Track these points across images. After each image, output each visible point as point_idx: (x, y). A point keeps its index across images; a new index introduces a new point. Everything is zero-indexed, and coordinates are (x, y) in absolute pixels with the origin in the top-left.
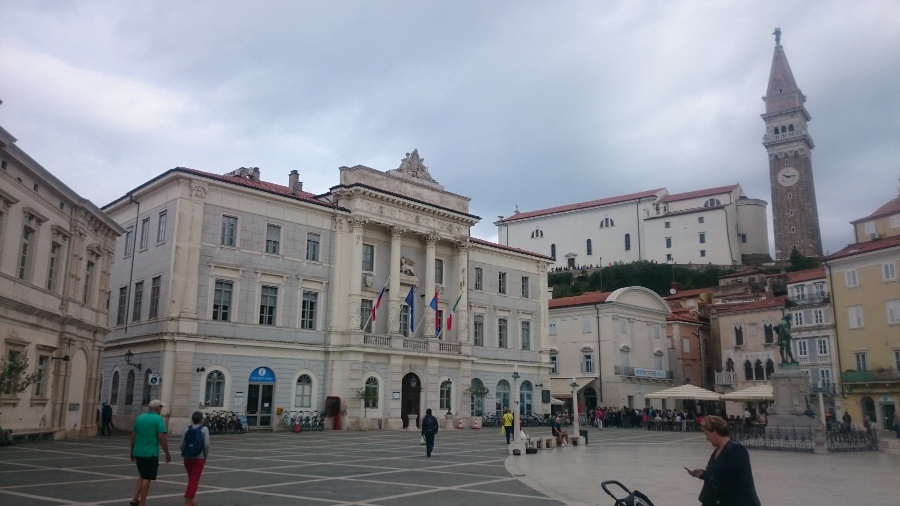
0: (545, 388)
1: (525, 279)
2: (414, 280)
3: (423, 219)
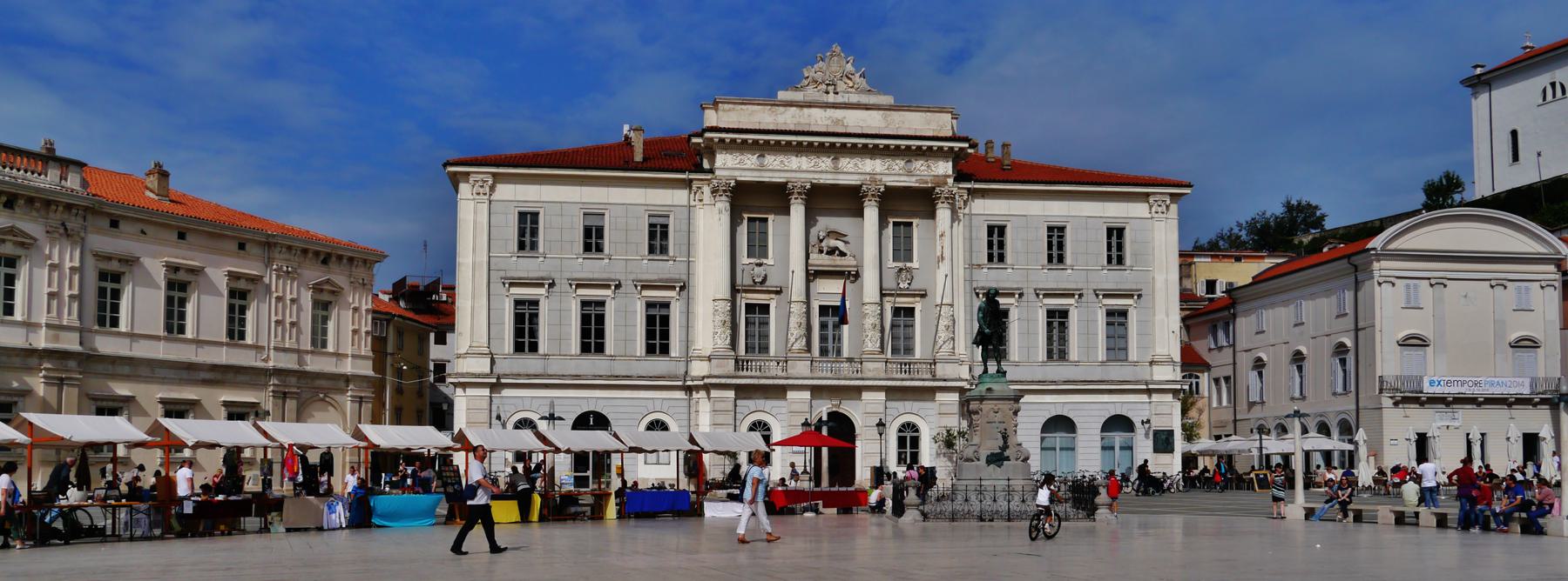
0: (1159, 424)
1: (1116, 234)
2: (847, 263)
3: (846, 163)
